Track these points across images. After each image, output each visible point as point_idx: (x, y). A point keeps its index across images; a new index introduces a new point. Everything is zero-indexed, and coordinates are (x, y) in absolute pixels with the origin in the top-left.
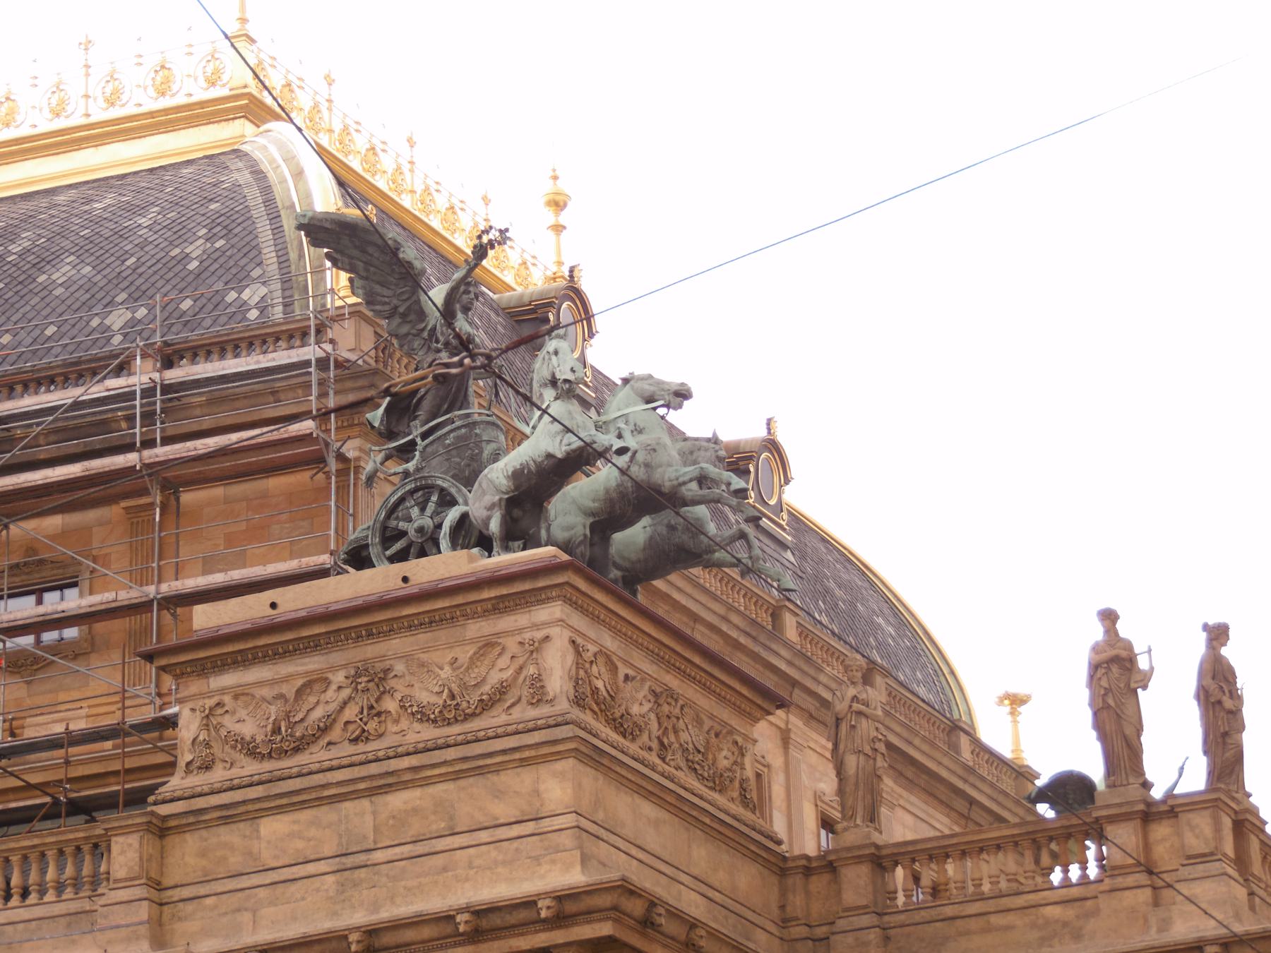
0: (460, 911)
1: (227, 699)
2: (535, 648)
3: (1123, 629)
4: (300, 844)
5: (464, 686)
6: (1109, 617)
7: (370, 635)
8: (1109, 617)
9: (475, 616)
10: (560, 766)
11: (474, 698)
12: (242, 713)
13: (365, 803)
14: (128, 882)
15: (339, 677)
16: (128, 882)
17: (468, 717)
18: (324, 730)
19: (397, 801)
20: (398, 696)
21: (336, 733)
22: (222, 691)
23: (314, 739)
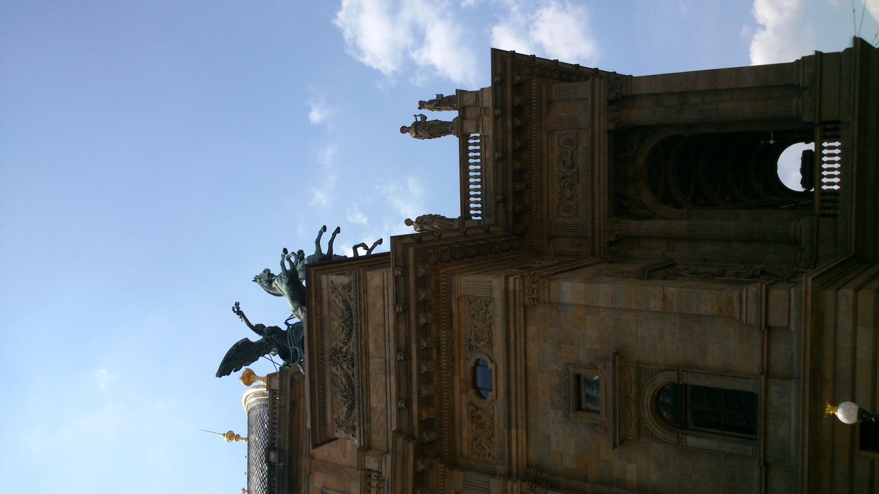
0: (395, 309)
1: (335, 416)
2: (334, 288)
3: (409, 125)
4: (381, 390)
5: (342, 317)
6: (404, 130)
7: (322, 354)
8: (404, 130)
9: (322, 310)
10: (369, 278)
11: (346, 313)
12: (340, 411)
13: (371, 361)
14: (380, 463)
15: (334, 369)
16: (380, 463)
17: (351, 316)
18: (348, 377)
19: (372, 347)
20: (341, 345)
21: (350, 373)
22: (332, 418)
23: (351, 382)
